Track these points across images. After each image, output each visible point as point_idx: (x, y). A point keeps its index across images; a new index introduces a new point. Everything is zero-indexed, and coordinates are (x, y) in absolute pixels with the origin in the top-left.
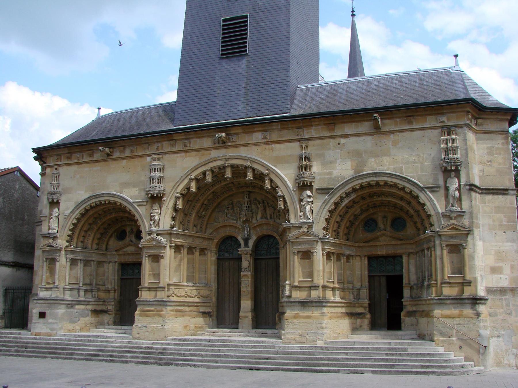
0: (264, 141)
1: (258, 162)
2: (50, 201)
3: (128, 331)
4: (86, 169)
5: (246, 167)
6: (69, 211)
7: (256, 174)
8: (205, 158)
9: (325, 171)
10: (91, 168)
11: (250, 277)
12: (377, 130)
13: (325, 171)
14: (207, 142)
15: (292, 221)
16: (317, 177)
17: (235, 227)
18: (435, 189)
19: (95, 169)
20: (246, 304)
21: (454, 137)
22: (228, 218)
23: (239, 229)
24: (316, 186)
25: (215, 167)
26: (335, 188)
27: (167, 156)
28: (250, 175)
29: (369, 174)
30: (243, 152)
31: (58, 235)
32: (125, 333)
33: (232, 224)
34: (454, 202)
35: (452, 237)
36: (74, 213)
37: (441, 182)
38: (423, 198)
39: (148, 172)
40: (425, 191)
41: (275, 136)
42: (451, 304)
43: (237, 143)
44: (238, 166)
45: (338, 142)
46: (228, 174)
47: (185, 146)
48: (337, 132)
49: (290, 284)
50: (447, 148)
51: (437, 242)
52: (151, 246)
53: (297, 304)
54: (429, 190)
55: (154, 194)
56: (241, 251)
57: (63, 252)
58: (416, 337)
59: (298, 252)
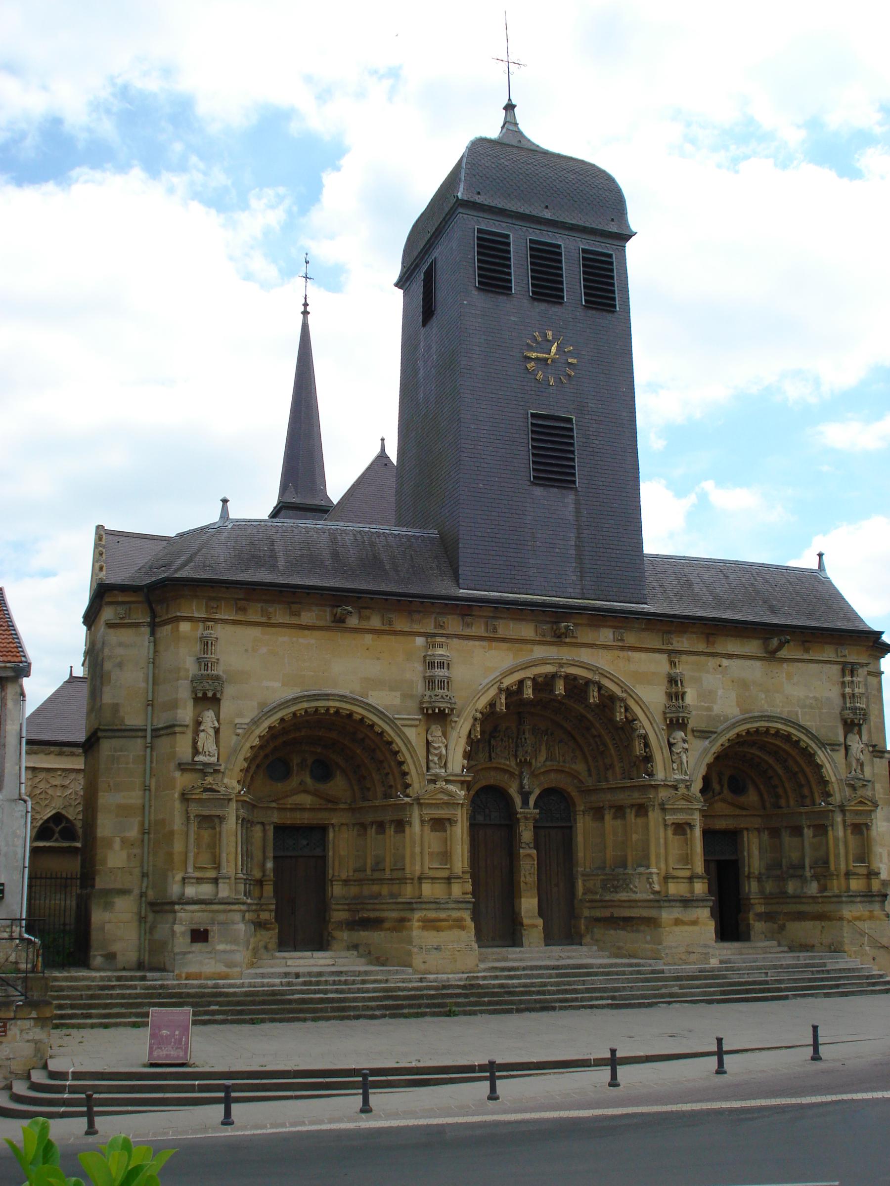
0: (620, 644)
1: (611, 677)
2: (200, 695)
3: (341, 960)
4: (283, 639)
5: (588, 682)
6: (247, 721)
7: (604, 695)
8: (524, 658)
9: (703, 704)
10: (295, 639)
11: (536, 859)
12: (771, 656)
13: (703, 704)
14: (527, 630)
15: (660, 775)
16: (694, 713)
17: (505, 771)
18: (837, 748)
19: (301, 640)
20: (528, 904)
21: (859, 679)
22: (496, 753)
23: (512, 774)
24: (690, 726)
25: (540, 675)
26: (719, 730)
27: (455, 642)
28: (594, 697)
29: (762, 717)
30: (585, 656)
31: (222, 768)
32: (333, 965)
33: (502, 766)
34: (857, 766)
35: (857, 813)
36: (258, 727)
37: (842, 739)
38: (821, 757)
39: (419, 667)
40: (825, 748)
41: (631, 638)
42: (861, 902)
43: (579, 641)
44: (575, 678)
45: (718, 663)
46: (560, 688)
47: (495, 630)
48: (719, 649)
49: (658, 874)
50: (853, 694)
51: (839, 819)
52: (438, 802)
53: (678, 904)
54: (830, 747)
55: (444, 710)
56: (521, 813)
57: (233, 805)
58: (786, 949)
59: (673, 824)
